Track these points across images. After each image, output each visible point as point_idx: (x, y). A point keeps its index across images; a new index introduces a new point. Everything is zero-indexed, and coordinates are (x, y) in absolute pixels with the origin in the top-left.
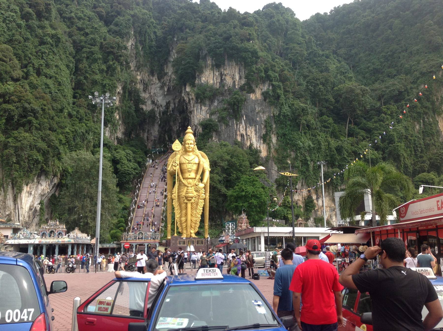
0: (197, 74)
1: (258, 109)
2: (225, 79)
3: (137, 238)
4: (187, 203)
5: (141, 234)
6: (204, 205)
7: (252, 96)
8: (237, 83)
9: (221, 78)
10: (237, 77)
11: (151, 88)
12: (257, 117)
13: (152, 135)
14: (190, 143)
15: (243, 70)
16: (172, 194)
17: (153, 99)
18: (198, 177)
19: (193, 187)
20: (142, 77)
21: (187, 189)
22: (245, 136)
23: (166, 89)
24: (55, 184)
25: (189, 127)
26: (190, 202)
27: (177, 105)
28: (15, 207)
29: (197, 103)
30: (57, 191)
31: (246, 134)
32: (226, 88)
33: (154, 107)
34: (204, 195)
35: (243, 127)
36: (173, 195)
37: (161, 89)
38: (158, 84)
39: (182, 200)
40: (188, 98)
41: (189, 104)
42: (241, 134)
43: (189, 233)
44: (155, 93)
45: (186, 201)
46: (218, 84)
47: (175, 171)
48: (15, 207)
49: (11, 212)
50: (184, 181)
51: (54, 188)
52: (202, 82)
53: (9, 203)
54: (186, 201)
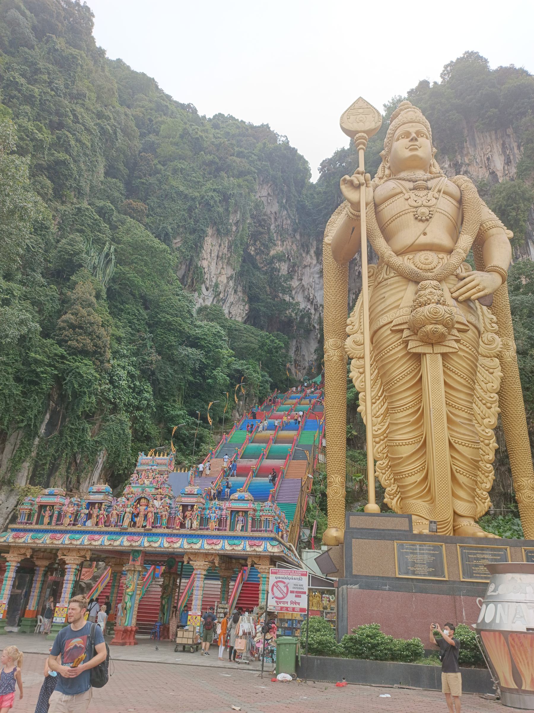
6: (503, 381)
8: (499, 174)
10: (498, 163)
11: (302, 274)
13: (304, 360)
14: (413, 130)
15: (515, 145)
17: (306, 293)
19: (445, 287)
20: (286, 249)
33: (309, 307)
34: (496, 337)
36: (349, 342)
38: (315, 265)
45: (414, 346)
50: (397, 261)
54: (414, 346)
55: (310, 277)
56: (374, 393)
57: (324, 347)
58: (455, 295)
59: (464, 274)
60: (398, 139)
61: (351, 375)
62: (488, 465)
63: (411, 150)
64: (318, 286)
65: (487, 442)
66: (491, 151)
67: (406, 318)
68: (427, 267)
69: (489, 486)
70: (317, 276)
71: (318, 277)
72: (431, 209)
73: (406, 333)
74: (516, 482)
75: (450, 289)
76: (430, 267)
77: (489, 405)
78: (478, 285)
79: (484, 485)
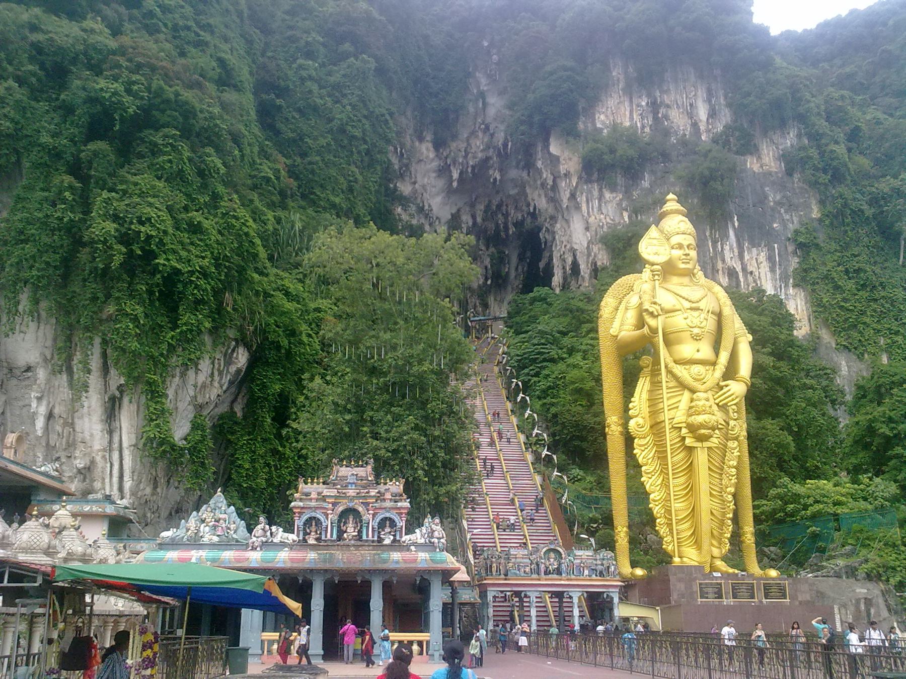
0: (582, 104)
1: (773, 197)
2: (666, 117)
3: (542, 567)
4: (690, 450)
5: (552, 555)
7: (752, 164)
9: (655, 113)
10: (702, 113)
11: (416, 171)
12: (774, 221)
14: (686, 243)
15: (721, 93)
16: (626, 417)
18: (724, 357)
19: (710, 394)
21: (692, 400)
22: (741, 275)
23: (455, 175)
24: (239, 371)
25: (671, 196)
26: (706, 444)
27: (479, 220)
28: (110, 442)
29: (589, 181)
30: (239, 400)
31: (744, 269)
32: (673, 140)
35: (731, 249)
36: (632, 424)
37: (439, 176)
38: (433, 160)
39: (670, 437)
40: (552, 174)
41: (551, 194)
42: (729, 269)
43: (709, 559)
44: (424, 187)
45: (689, 442)
46: (647, 130)
47: (654, 331)
48: (110, 442)
49: (93, 462)
50: (679, 370)
51: (233, 390)
52: (599, 125)
53: (87, 425)
54: (689, 442)
55: (424, 176)
56: (654, 467)
57: (608, 422)
58: (717, 401)
59: (722, 384)
60: (672, 248)
61: (635, 452)
62: (729, 521)
63: (683, 263)
64: (434, 189)
65: (728, 505)
66: (695, 95)
67: (683, 419)
68: (698, 377)
69: (729, 536)
70: (434, 175)
71: (435, 178)
72: (703, 330)
73: (684, 431)
74: (742, 529)
75: (713, 395)
76: (702, 377)
77: (730, 477)
78: (733, 394)
79: (726, 535)
